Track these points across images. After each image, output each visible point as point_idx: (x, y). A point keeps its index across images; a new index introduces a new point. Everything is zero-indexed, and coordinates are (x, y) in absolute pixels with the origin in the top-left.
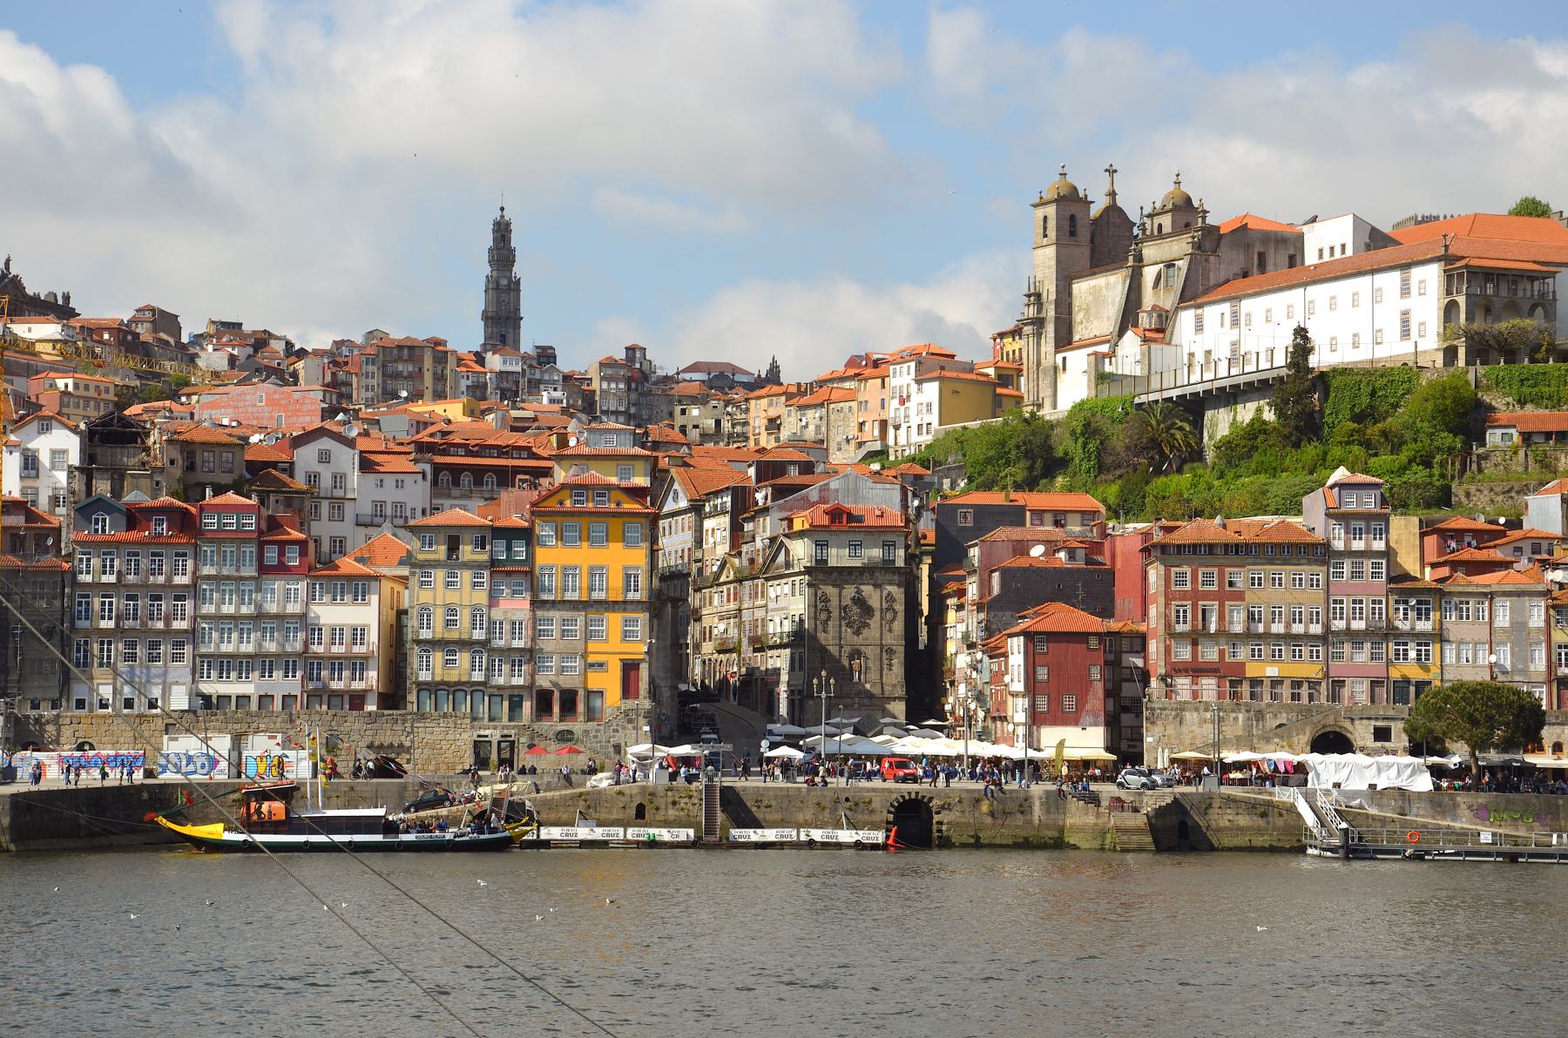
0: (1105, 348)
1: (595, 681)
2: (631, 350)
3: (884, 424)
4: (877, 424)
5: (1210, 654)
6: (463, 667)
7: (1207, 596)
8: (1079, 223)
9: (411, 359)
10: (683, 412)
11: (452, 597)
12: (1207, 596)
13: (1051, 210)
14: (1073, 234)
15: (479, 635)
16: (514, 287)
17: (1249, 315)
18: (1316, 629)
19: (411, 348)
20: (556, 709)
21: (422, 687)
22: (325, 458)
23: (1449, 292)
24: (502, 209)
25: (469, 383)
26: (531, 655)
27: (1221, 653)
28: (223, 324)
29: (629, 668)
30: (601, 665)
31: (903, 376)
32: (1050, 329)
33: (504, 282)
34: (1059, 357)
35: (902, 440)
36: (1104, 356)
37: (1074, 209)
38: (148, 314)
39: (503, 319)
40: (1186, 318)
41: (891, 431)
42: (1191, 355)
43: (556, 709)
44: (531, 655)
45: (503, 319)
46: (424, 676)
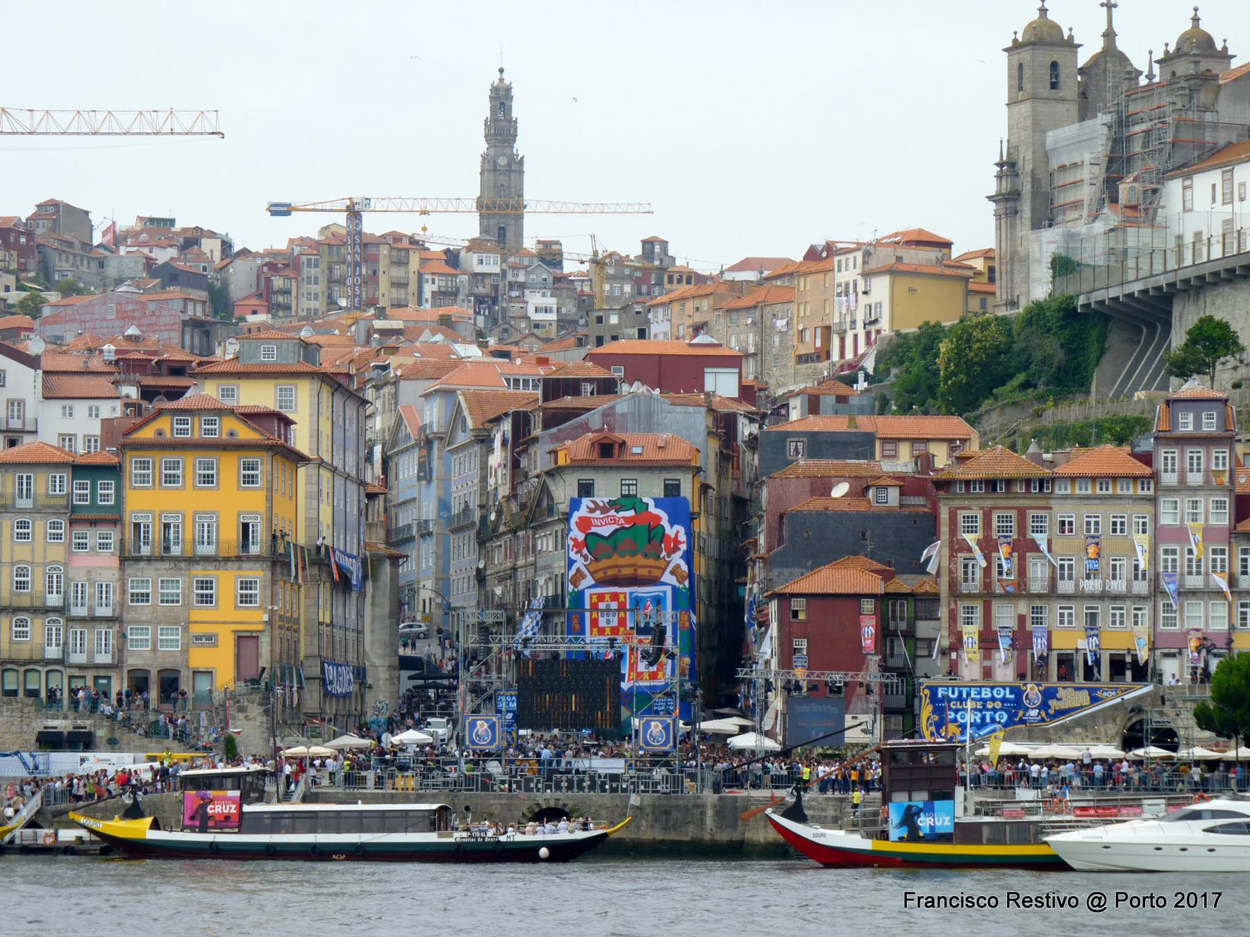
1: (200, 658)
2: (648, 244)
4: (819, 331)
8: (1063, 72)
15: (54, 600)
16: (515, 167)
17: (1243, 185)
18: (1141, 587)
24: (501, 71)
25: (435, 288)
28: (152, 220)
30: (209, 638)
32: (1026, 207)
33: (502, 161)
37: (1056, 55)
38: (51, 210)
42: (1180, 237)
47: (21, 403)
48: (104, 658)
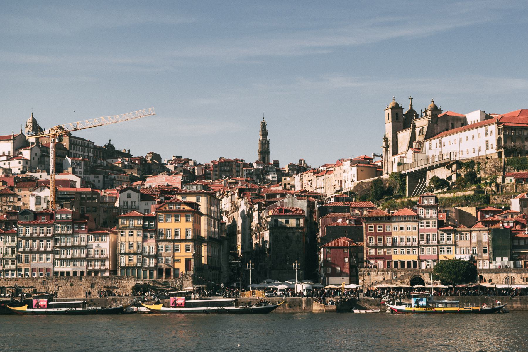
0: (404, 155)
1: (177, 265)
3: (341, 181)
5: (381, 252)
6: (135, 260)
7: (380, 234)
8: (399, 115)
9: (228, 166)
10: (285, 179)
11: (131, 239)
12: (380, 234)
13: (390, 111)
14: (397, 119)
15: (139, 251)
17: (444, 143)
18: (415, 244)
19: (229, 162)
20: (164, 275)
21: (123, 268)
22: (129, 196)
23: (499, 134)
26: (157, 256)
27: (384, 252)
28: (176, 157)
29: (187, 261)
31: (346, 165)
32: (390, 149)
34: (394, 158)
35: (347, 187)
36: (403, 157)
38: (151, 155)
39: (265, 152)
40: (427, 143)
41: (343, 183)
43: (164, 275)
44: (157, 256)
45: (265, 152)
46: (123, 265)
47: (135, 202)
48: (152, 265)
